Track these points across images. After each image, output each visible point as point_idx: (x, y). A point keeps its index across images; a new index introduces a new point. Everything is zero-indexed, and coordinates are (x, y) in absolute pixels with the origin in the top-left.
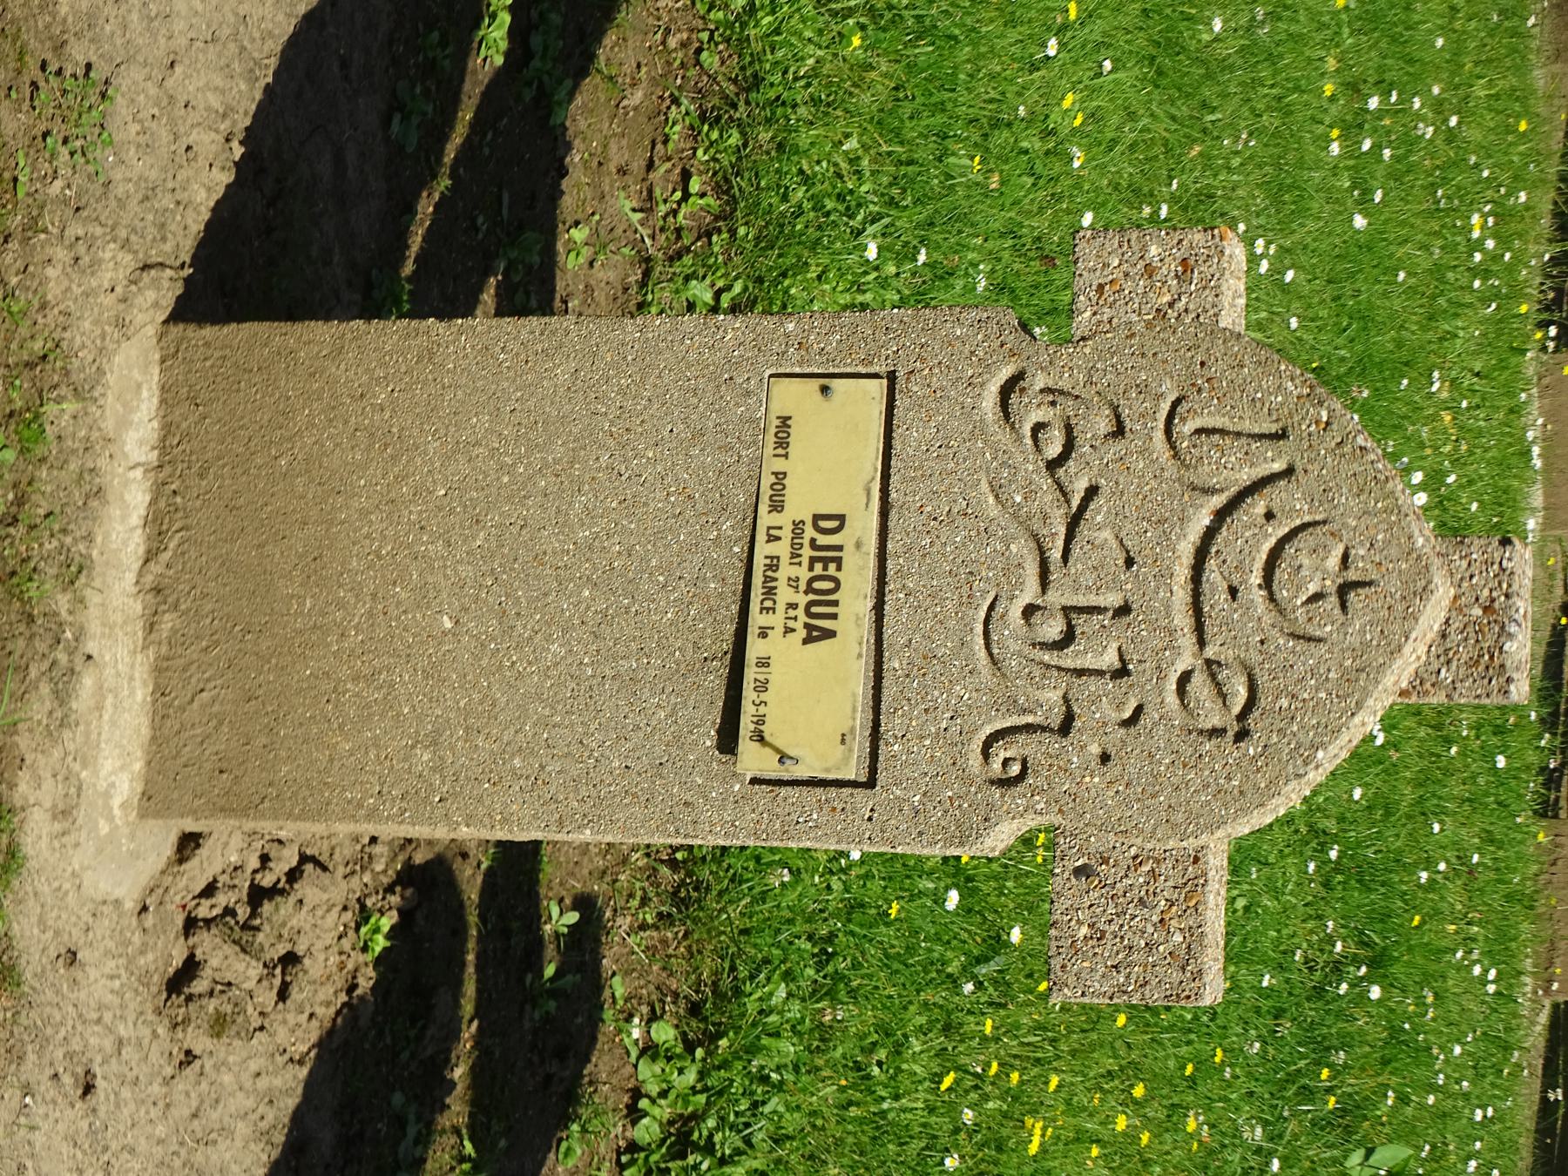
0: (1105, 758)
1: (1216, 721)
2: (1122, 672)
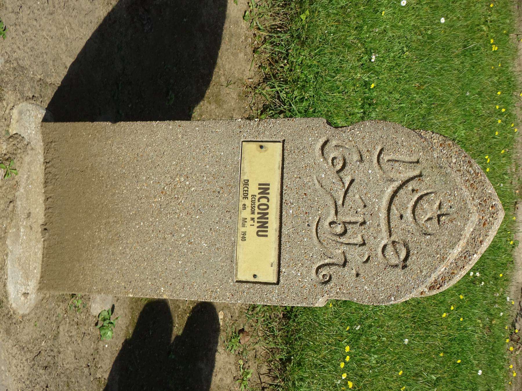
0: (358, 275)
1: (394, 261)
2: (364, 244)
